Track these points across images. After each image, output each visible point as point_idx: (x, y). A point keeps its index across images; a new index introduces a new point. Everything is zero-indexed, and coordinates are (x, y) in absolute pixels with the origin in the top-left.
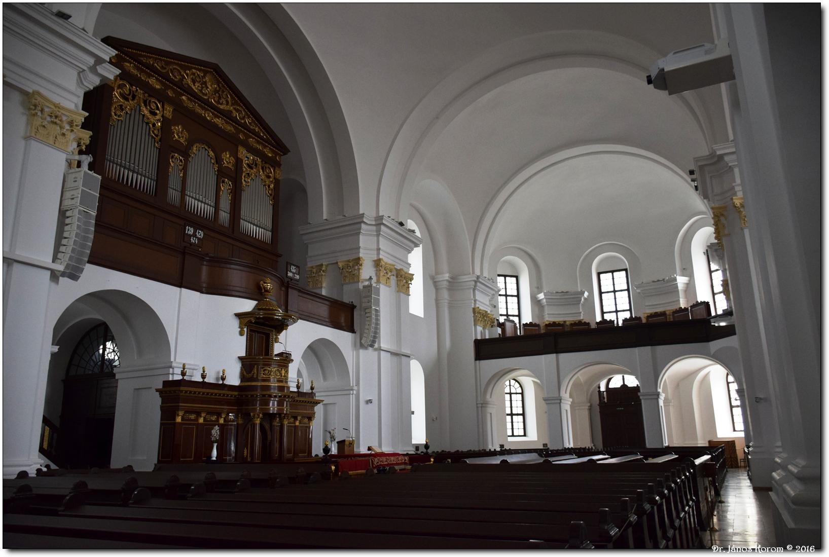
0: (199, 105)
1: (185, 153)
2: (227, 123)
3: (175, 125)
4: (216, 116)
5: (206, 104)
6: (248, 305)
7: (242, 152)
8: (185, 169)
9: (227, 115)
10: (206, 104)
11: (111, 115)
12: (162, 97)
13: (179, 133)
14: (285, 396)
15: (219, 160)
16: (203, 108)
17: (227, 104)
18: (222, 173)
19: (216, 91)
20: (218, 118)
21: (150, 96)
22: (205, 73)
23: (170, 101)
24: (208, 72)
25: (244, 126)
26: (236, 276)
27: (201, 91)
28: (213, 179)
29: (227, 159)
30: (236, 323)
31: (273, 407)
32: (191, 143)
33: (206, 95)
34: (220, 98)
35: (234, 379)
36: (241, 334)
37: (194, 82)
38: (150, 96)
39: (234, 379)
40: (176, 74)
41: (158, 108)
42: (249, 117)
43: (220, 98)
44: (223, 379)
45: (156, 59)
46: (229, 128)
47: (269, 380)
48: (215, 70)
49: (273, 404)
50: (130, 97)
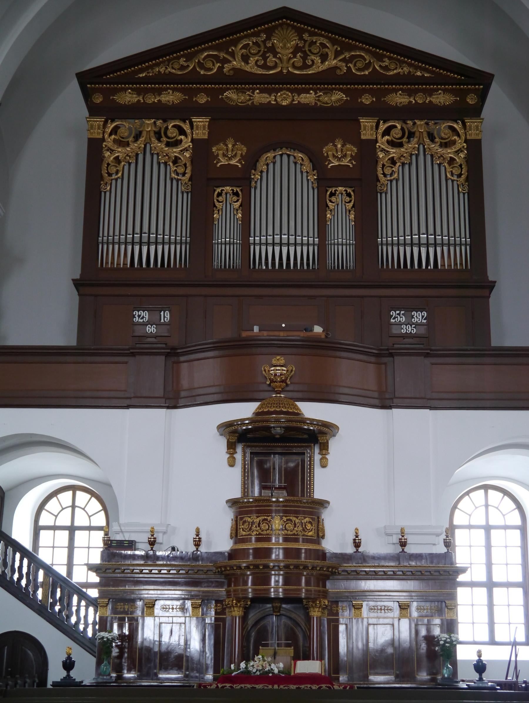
0: (262, 91)
1: (242, 180)
2: (327, 92)
3: (217, 143)
4: (299, 92)
5: (284, 81)
6: (244, 411)
7: (367, 128)
8: (246, 207)
9: (326, 80)
10: (284, 81)
11: (102, 178)
12: (185, 112)
13: (229, 154)
14: (297, 567)
15: (318, 162)
16: (269, 92)
17: (324, 58)
18: (327, 181)
19: (297, 50)
20: (307, 91)
21: (165, 121)
22: (270, 33)
23: (201, 111)
24: (276, 27)
25: (376, 78)
26: (205, 370)
27: (265, 67)
28: (308, 197)
29: (340, 155)
30: (222, 443)
31: (276, 584)
32: (251, 162)
33: (275, 67)
34: (305, 58)
35: (220, 542)
36: (232, 463)
37: (245, 59)
38: (165, 121)
39: (220, 542)
40: (209, 65)
41: (182, 132)
42: (380, 58)
43: (305, 58)
44: (197, 543)
45: (169, 61)
46: (337, 97)
47: (269, 540)
48: (285, 17)
49: (277, 582)
50: (131, 139)
